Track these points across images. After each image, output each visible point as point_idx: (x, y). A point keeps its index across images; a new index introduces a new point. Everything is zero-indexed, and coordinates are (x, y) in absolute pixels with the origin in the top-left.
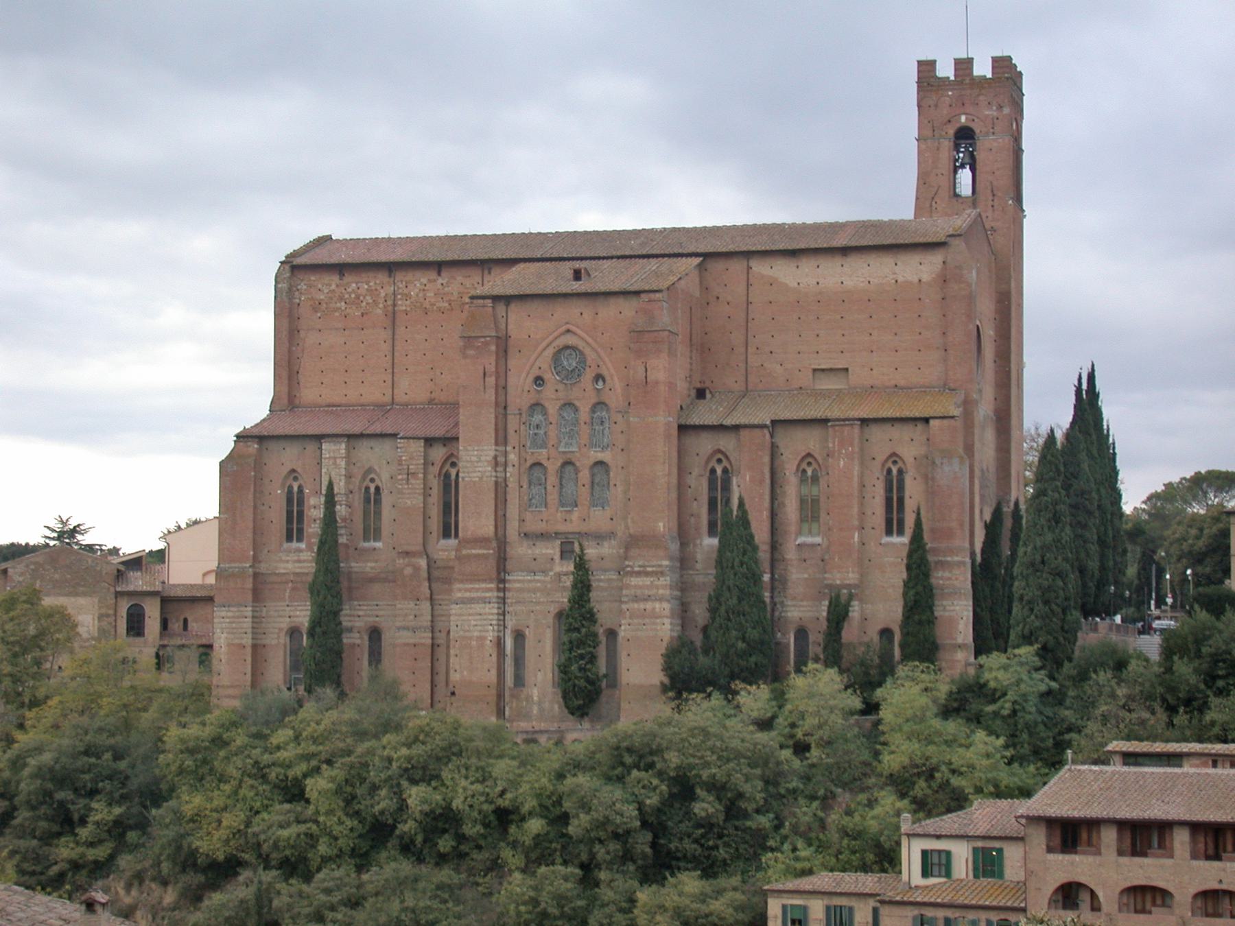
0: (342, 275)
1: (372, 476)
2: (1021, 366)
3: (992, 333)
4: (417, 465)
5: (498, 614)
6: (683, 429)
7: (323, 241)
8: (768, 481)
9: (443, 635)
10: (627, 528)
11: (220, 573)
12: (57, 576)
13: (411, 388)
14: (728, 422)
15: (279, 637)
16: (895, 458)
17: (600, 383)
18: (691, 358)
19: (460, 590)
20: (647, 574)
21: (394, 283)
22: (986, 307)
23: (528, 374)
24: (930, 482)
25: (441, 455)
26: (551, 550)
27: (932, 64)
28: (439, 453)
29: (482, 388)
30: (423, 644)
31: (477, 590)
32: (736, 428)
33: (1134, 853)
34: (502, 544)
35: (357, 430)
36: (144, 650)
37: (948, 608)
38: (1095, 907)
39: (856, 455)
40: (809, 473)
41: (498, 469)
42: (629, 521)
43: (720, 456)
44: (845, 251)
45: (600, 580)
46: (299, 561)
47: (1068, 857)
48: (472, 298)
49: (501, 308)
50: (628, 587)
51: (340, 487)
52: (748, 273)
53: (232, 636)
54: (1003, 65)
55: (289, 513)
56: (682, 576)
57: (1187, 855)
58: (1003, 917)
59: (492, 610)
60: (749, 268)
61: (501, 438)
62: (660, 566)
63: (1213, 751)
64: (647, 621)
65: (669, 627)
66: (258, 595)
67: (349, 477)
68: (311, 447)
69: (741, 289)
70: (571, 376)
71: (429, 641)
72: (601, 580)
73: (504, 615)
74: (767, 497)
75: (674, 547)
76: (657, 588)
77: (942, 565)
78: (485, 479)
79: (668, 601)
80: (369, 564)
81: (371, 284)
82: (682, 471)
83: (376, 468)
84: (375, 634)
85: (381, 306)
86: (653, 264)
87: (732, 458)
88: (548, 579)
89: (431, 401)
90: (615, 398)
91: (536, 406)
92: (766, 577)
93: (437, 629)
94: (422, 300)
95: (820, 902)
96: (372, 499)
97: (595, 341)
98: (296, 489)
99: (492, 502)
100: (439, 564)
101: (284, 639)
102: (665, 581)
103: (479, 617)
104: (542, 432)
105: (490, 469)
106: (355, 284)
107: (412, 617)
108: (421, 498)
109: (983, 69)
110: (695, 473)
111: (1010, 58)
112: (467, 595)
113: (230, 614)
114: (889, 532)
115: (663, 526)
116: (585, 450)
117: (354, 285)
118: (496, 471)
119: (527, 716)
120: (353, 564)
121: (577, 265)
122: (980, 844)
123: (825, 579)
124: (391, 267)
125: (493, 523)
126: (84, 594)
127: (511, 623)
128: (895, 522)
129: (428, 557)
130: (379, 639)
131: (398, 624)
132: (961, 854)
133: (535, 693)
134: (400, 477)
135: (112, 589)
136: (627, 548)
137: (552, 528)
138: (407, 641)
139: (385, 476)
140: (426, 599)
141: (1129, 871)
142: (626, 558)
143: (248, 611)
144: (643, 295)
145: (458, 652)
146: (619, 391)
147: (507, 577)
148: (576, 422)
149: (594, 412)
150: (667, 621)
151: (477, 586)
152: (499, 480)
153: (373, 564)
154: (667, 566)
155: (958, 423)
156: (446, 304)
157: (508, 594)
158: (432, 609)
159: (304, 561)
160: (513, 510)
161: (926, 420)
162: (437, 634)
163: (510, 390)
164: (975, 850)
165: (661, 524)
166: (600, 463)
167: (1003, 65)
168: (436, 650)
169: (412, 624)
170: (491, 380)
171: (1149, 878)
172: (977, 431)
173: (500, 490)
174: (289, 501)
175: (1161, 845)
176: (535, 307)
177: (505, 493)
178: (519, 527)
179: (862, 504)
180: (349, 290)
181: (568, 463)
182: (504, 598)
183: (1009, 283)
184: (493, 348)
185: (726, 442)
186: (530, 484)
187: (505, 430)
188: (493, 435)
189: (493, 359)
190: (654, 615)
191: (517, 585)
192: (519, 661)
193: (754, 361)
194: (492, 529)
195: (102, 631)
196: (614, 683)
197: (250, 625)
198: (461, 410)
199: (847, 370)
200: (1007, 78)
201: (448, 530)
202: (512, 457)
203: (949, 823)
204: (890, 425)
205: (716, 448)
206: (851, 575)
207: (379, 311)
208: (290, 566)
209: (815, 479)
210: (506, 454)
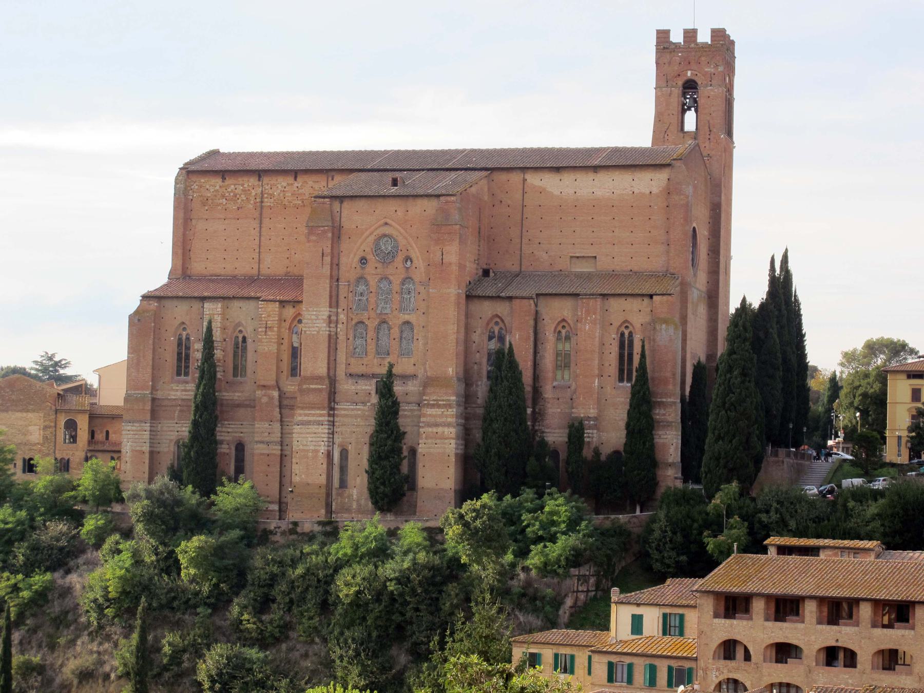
0: (224, 179)
1: (240, 328)
2: (728, 258)
3: (706, 233)
4: (273, 321)
5: (329, 433)
6: (469, 297)
7: (214, 154)
8: (532, 339)
10: (426, 371)
12: (13, 397)
13: (272, 265)
14: (503, 294)
15: (169, 447)
16: (626, 324)
18: (479, 246)
19: (300, 415)
20: (439, 406)
21: (262, 186)
23: (355, 255)
24: (652, 343)
25: (291, 314)
26: (370, 387)
27: (667, 32)
28: (290, 312)
29: (320, 265)
30: (274, 455)
31: (314, 415)
32: (510, 298)
33: (777, 619)
34: (332, 381)
35: (230, 294)
36: (76, 453)
37: (662, 437)
38: (747, 657)
39: (598, 321)
41: (331, 325)
42: (427, 366)
43: (498, 320)
44: (596, 169)
46: (186, 390)
47: (728, 621)
49: (336, 205)
50: (425, 415)
51: (217, 335)
52: (524, 184)
53: (135, 444)
54: (719, 35)
55: (179, 354)
56: (466, 408)
57: (814, 621)
58: (680, 664)
59: (324, 430)
60: (525, 180)
61: (334, 301)
62: (449, 400)
63: (841, 545)
64: (438, 441)
65: (454, 446)
66: (154, 415)
67: (224, 329)
68: (196, 305)
69: (519, 196)
70: (387, 258)
71: (279, 452)
72: (406, 410)
73: (333, 434)
74: (532, 351)
75: (461, 388)
76: (447, 416)
77: (661, 404)
78: (321, 332)
79: (454, 427)
80: (237, 394)
81: (246, 186)
82: (468, 330)
83: (243, 322)
84: (240, 448)
85: (252, 202)
86: (453, 175)
87: (506, 322)
88: (366, 408)
89: (287, 274)
91: (361, 279)
92: (529, 411)
93: (285, 444)
94: (282, 198)
95: (551, 650)
96: (240, 346)
97: (406, 231)
98: (184, 337)
100: (287, 395)
101: (173, 448)
102: (453, 411)
103: (314, 435)
104: (365, 298)
105: (325, 325)
106: (234, 185)
107: (266, 434)
108: (275, 346)
109: (704, 37)
110: (479, 331)
111: (724, 31)
112: (306, 418)
113: (134, 428)
114: (621, 380)
115: (451, 370)
116: (396, 312)
117: (233, 186)
118: (330, 327)
119: (348, 510)
120: (224, 394)
121: (397, 175)
122: (668, 610)
123: (572, 412)
124: (260, 174)
125: (326, 365)
126: (34, 411)
127: (338, 439)
128: (626, 372)
129: (279, 389)
130: (243, 450)
131: (256, 439)
133: (355, 492)
134: (260, 330)
135: (54, 408)
136: (425, 385)
137: (370, 371)
138: (263, 452)
140: (277, 421)
141: (772, 632)
142: (424, 394)
143: (147, 426)
144: (441, 198)
145: (298, 461)
146: (423, 269)
147: (336, 406)
148: (390, 292)
149: (403, 284)
150: (453, 442)
151: (313, 412)
152: (332, 333)
153: (240, 394)
154: (454, 401)
157: (336, 419)
158: (282, 429)
159: (189, 391)
160: (341, 357)
161: (651, 296)
162: (285, 448)
164: (665, 616)
165: (450, 370)
166: (407, 323)
167: (719, 35)
169: (267, 439)
170: (328, 259)
171: (787, 637)
172: (690, 306)
174: (180, 344)
175: (797, 614)
176: (361, 204)
177: (336, 344)
178: (346, 368)
179: (601, 359)
180: (229, 190)
181: (384, 322)
182: (333, 422)
183: (720, 197)
184: (330, 235)
185: (502, 308)
186: (355, 337)
187: (338, 296)
188: (328, 300)
189: (329, 243)
190: (443, 438)
191: (343, 412)
192: (343, 469)
193: (527, 250)
195: (46, 438)
196: (413, 487)
197: (148, 437)
198: (305, 281)
199: (595, 257)
200: (722, 45)
201: (294, 371)
202: (342, 317)
203: (647, 594)
204: (624, 299)
205: (495, 313)
206: (592, 411)
207: (251, 206)
209: (568, 338)
210: (337, 314)
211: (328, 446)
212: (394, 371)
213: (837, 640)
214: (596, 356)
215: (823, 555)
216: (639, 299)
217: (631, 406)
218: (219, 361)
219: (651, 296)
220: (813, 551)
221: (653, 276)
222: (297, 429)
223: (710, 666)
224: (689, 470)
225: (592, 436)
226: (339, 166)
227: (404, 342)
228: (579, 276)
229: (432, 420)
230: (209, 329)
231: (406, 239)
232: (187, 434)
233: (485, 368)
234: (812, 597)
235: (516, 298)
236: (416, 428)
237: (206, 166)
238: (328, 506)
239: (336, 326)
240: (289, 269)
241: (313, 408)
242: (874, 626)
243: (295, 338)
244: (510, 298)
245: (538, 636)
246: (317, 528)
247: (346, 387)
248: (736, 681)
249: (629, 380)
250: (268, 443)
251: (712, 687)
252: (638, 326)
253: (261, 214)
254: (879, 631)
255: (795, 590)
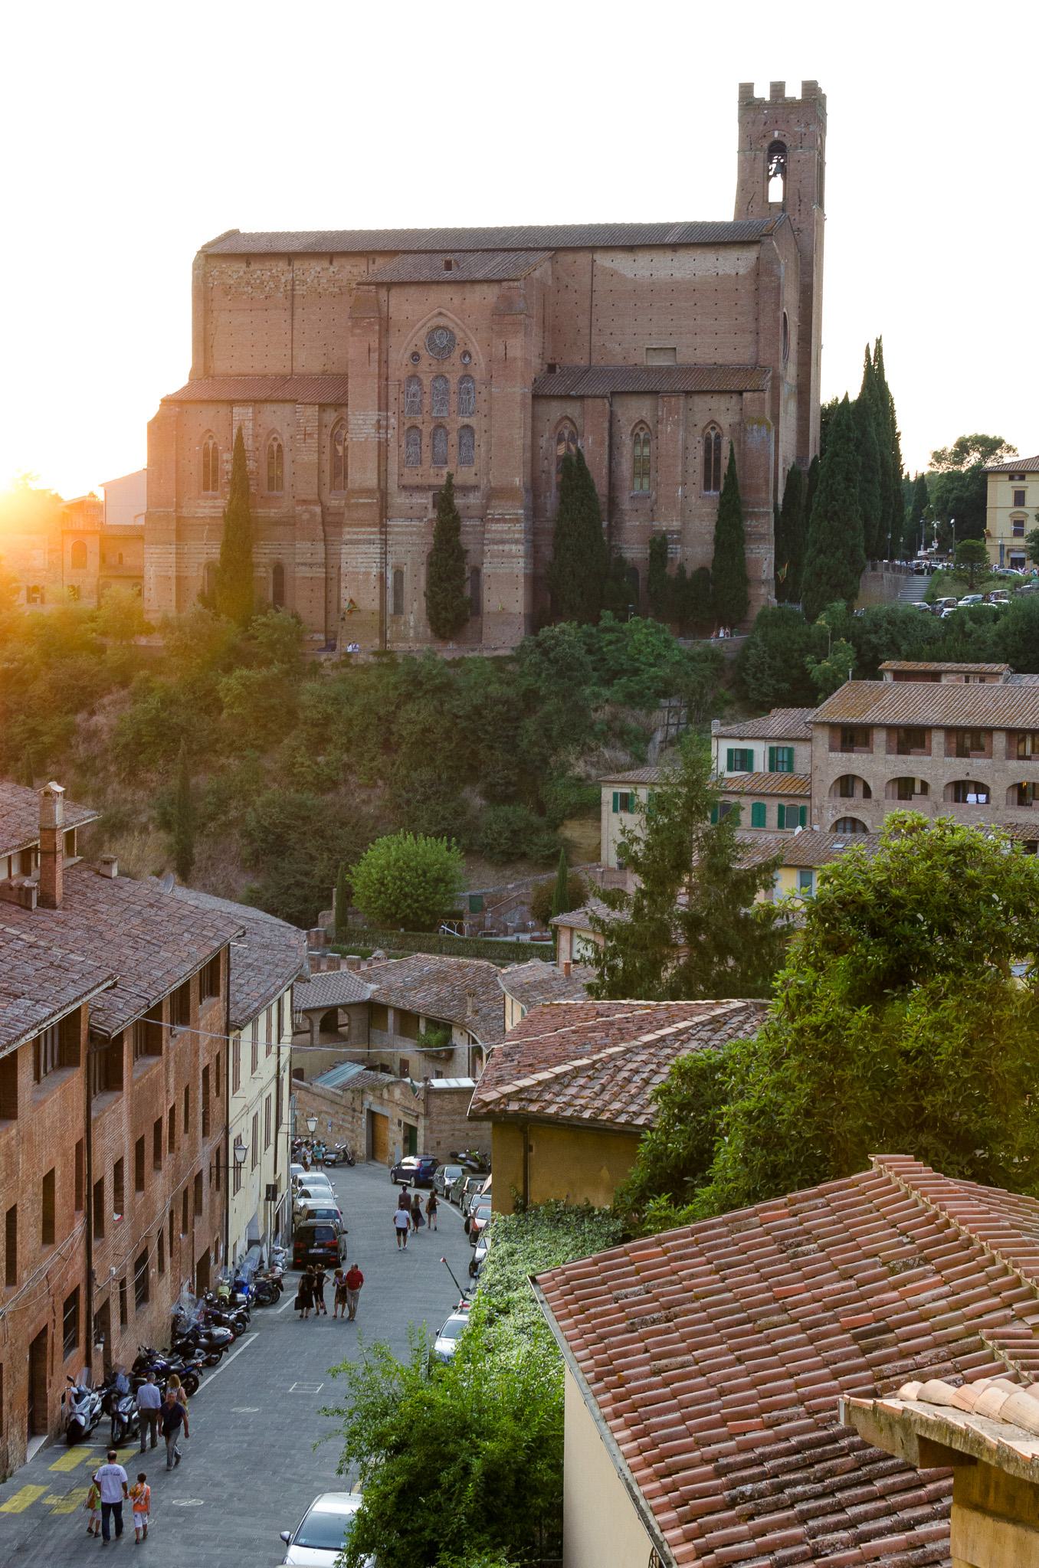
0: (248, 264)
2: (820, 347)
6: (536, 397)
7: (233, 235)
8: (607, 443)
9: (335, 570)
10: (489, 481)
11: (149, 516)
13: (308, 361)
17: (467, 359)
19: (349, 533)
20: (505, 521)
22: (790, 297)
26: (425, 500)
28: (331, 416)
32: (582, 397)
34: (384, 494)
35: (262, 395)
38: (867, 793)
40: (642, 437)
44: (675, 247)
45: (466, 526)
46: (214, 507)
47: (845, 755)
48: (359, 284)
49: (383, 293)
51: (249, 443)
55: (206, 465)
57: (942, 753)
59: (375, 549)
61: (383, 405)
64: (504, 560)
66: (180, 536)
67: (256, 436)
69: (587, 279)
72: (468, 525)
76: (514, 532)
82: (535, 434)
84: (279, 570)
89: (324, 373)
90: (479, 372)
91: (414, 378)
92: (605, 524)
96: (276, 455)
99: (376, 459)
104: (418, 400)
108: (316, 456)
109: (794, 92)
110: (546, 436)
112: (355, 537)
114: (707, 487)
115: (518, 481)
116: (454, 416)
119: (405, 639)
121: (449, 257)
122: (775, 744)
124: (290, 257)
127: (391, 560)
131: (298, 561)
132: (760, 752)
133: (412, 618)
139: (286, 437)
142: (487, 508)
143: (173, 549)
144: (504, 284)
148: (447, 392)
149: (461, 383)
150: (521, 560)
155: (767, 395)
156: (337, 290)
160: (393, 467)
161: (740, 393)
162: (330, 570)
163: (392, 365)
164: (771, 749)
165: (517, 479)
166: (467, 427)
168: (331, 580)
169: (309, 561)
170: (375, 356)
172: (781, 403)
173: (383, 448)
174: (206, 455)
179: (684, 464)
181: (440, 426)
182: (386, 540)
184: (377, 327)
185: (572, 409)
189: (376, 338)
191: (396, 529)
194: (375, 482)
202: (393, 421)
206: (675, 523)
208: (207, 511)
210: (387, 418)
211: (381, 567)
212: (454, 482)
213: (968, 774)
214: (679, 462)
215: (944, 681)
216: (728, 396)
217: (719, 517)
218: (252, 473)
219: (740, 393)
220: (935, 676)
221: (740, 370)
222: (345, 549)
223: (826, 805)
224: (782, 590)
225: (677, 552)
226: (379, 247)
227: (464, 448)
228: (659, 370)
229: (498, 536)
230: (240, 437)
231: (464, 331)
232: (219, 556)
233: (554, 478)
234: (939, 727)
235: (589, 397)
236: (479, 546)
237: (225, 248)
238: (382, 635)
239: (387, 433)
240: (326, 368)
241: (362, 525)
242: (1009, 757)
243: (340, 448)
244: (582, 397)
245: (631, 775)
246: (372, 659)
247: (399, 500)
248: (854, 821)
249: (716, 488)
250: (311, 565)
251: (828, 828)
252: (725, 425)
253: (292, 304)
254: (1014, 764)
255: (919, 720)
